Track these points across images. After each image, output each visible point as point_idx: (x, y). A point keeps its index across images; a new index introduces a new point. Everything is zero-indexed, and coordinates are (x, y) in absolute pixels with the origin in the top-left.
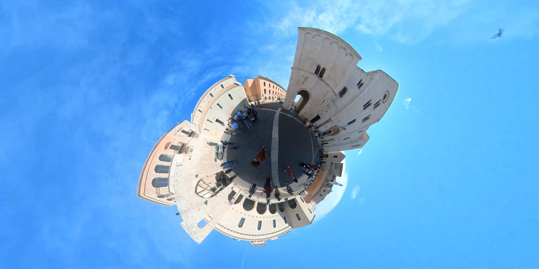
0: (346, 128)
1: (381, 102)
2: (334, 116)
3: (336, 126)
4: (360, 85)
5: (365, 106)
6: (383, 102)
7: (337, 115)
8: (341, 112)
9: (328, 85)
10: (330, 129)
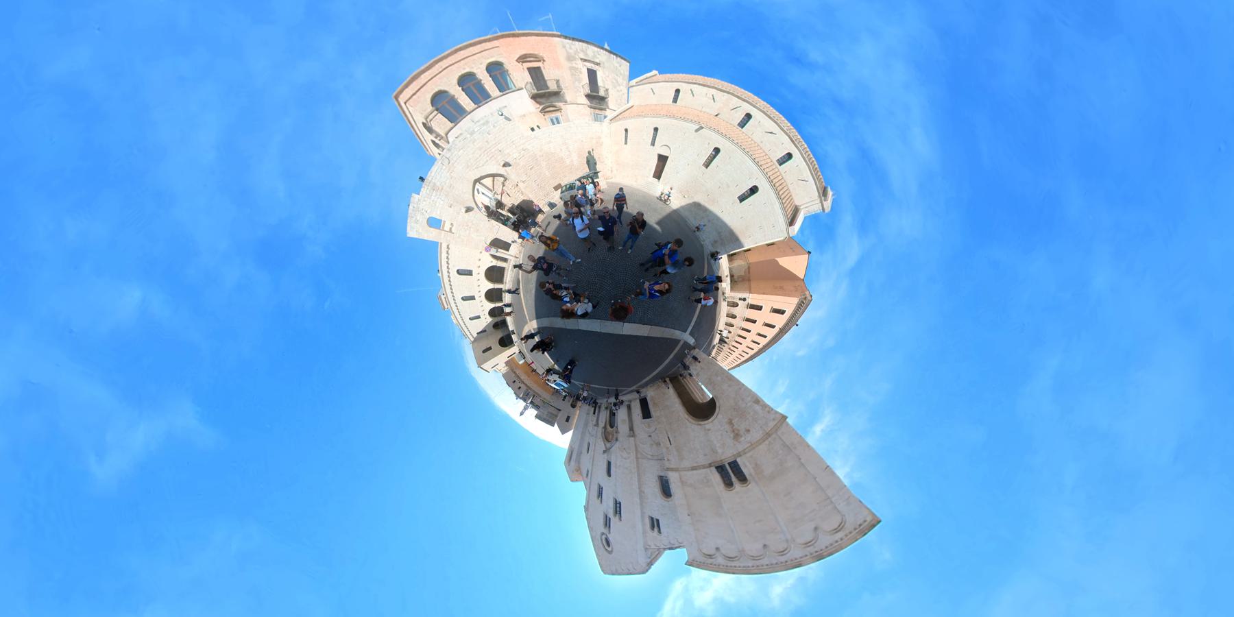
0: (605, 455)
1: (606, 531)
2: (636, 445)
3: (617, 440)
4: (655, 524)
5: (618, 505)
6: (603, 534)
7: (635, 452)
8: (635, 461)
9: (693, 469)
10: (617, 427)
